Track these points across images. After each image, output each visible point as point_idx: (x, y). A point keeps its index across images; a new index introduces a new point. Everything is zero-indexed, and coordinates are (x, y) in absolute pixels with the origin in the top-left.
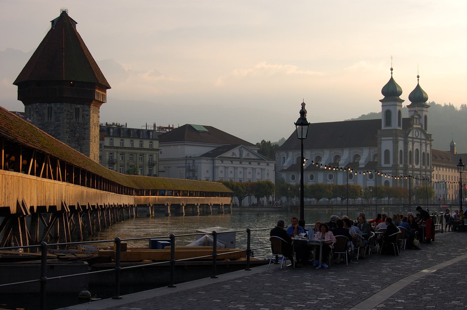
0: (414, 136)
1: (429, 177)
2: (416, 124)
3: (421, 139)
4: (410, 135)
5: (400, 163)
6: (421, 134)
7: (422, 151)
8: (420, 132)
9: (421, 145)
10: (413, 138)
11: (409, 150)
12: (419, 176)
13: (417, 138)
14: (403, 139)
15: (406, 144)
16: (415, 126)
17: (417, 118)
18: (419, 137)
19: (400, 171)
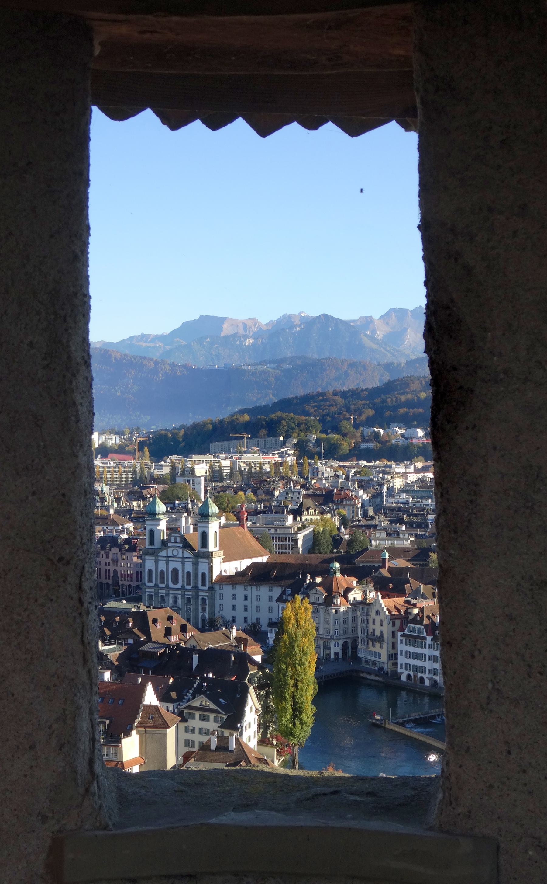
0: (170, 554)
1: (206, 598)
2: (175, 542)
3: (183, 558)
4: (164, 553)
5: (148, 582)
6: (183, 553)
7: (186, 571)
8: (180, 551)
9: (183, 565)
10: (167, 557)
11: (159, 569)
12: (179, 596)
13: (175, 557)
14: (154, 558)
15: (157, 562)
16: (169, 544)
17: (175, 537)
18: (180, 555)
19: (147, 590)
